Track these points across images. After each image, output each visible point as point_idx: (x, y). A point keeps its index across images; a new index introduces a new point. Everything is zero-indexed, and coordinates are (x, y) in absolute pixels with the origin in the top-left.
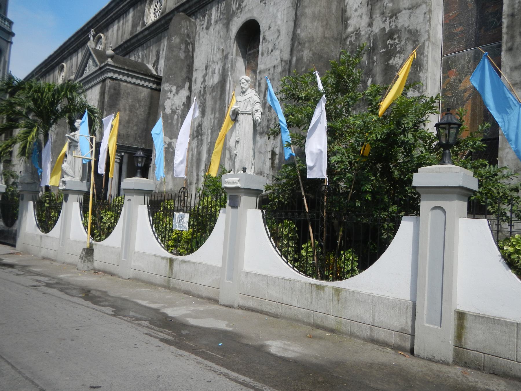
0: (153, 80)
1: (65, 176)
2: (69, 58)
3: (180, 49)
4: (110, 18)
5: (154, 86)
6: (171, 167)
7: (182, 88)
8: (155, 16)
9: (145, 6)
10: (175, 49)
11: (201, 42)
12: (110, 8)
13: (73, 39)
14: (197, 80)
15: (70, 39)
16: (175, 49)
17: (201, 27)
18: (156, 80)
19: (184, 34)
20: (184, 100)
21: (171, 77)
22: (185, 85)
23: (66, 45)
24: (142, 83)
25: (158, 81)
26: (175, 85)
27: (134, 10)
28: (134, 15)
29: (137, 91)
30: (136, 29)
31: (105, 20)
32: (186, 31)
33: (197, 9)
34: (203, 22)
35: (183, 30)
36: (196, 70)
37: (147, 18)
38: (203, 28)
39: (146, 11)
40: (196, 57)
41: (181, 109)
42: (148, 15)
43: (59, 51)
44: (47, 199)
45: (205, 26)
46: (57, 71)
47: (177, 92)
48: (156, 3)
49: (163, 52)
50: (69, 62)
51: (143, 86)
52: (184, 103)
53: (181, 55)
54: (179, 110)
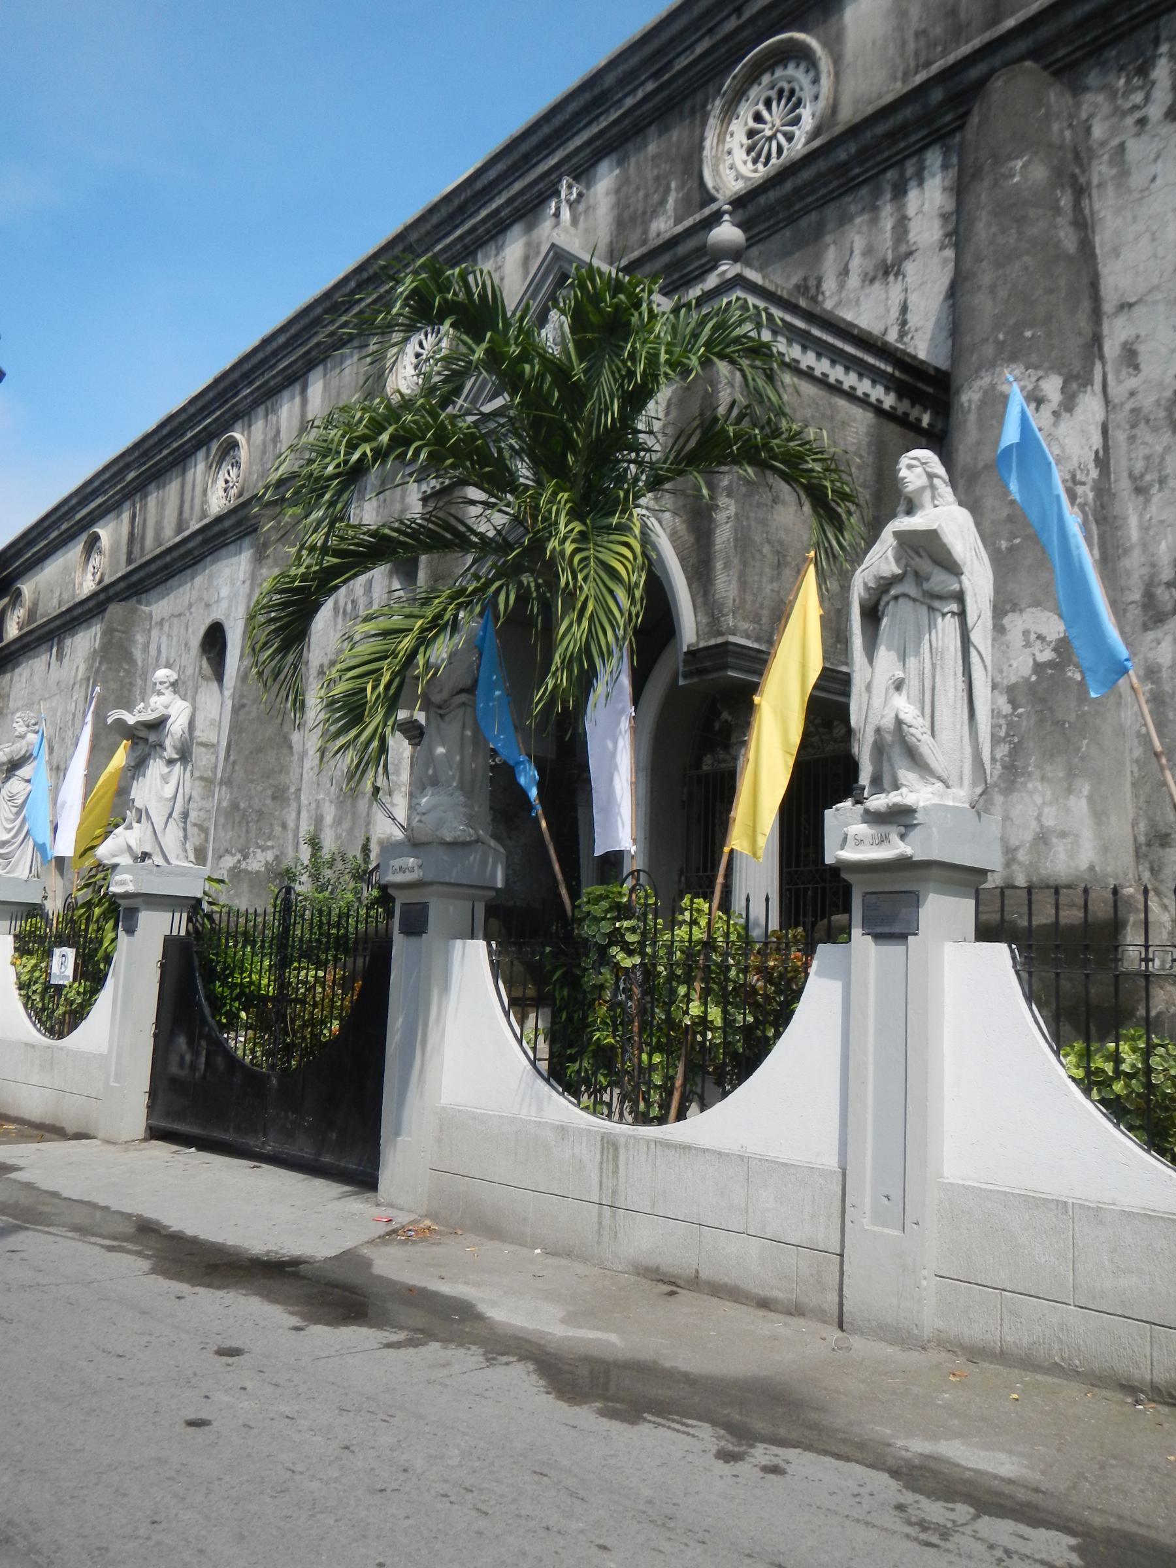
0: (889, 369)
1: (907, 776)
2: (261, 410)
3: (1057, 210)
4: (484, 221)
5: (889, 401)
6: (1082, 758)
7: (1085, 386)
8: (755, 161)
9: (704, 124)
10: (1032, 212)
11: (1137, 180)
12: (479, 185)
13: (282, 339)
14: (1142, 348)
15: (266, 342)
16: (1032, 212)
17: (1130, 120)
18: (897, 374)
19: (1061, 147)
20: (1096, 441)
21: (1028, 334)
22: (1092, 370)
23: (247, 366)
24: (850, 380)
25: (903, 377)
26: (1055, 368)
27: (620, 163)
28: (624, 181)
29: (832, 418)
30: (646, 231)
31: (458, 232)
32: (1068, 134)
33: (1079, 54)
34: (1138, 98)
35: (1056, 127)
36: (1125, 307)
37: (716, 172)
38: (1142, 122)
39: (707, 144)
40: (1116, 252)
41: (1090, 483)
42: (717, 160)
43: (211, 395)
44: (626, 924)
45: (1155, 111)
46: (201, 467)
47: (1068, 404)
48: (761, 107)
49: (842, 286)
50: (258, 426)
51: (850, 395)
52: (1097, 452)
53: (1062, 234)
54: (1083, 484)
